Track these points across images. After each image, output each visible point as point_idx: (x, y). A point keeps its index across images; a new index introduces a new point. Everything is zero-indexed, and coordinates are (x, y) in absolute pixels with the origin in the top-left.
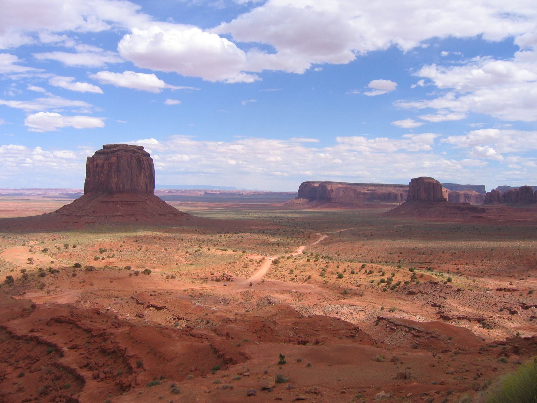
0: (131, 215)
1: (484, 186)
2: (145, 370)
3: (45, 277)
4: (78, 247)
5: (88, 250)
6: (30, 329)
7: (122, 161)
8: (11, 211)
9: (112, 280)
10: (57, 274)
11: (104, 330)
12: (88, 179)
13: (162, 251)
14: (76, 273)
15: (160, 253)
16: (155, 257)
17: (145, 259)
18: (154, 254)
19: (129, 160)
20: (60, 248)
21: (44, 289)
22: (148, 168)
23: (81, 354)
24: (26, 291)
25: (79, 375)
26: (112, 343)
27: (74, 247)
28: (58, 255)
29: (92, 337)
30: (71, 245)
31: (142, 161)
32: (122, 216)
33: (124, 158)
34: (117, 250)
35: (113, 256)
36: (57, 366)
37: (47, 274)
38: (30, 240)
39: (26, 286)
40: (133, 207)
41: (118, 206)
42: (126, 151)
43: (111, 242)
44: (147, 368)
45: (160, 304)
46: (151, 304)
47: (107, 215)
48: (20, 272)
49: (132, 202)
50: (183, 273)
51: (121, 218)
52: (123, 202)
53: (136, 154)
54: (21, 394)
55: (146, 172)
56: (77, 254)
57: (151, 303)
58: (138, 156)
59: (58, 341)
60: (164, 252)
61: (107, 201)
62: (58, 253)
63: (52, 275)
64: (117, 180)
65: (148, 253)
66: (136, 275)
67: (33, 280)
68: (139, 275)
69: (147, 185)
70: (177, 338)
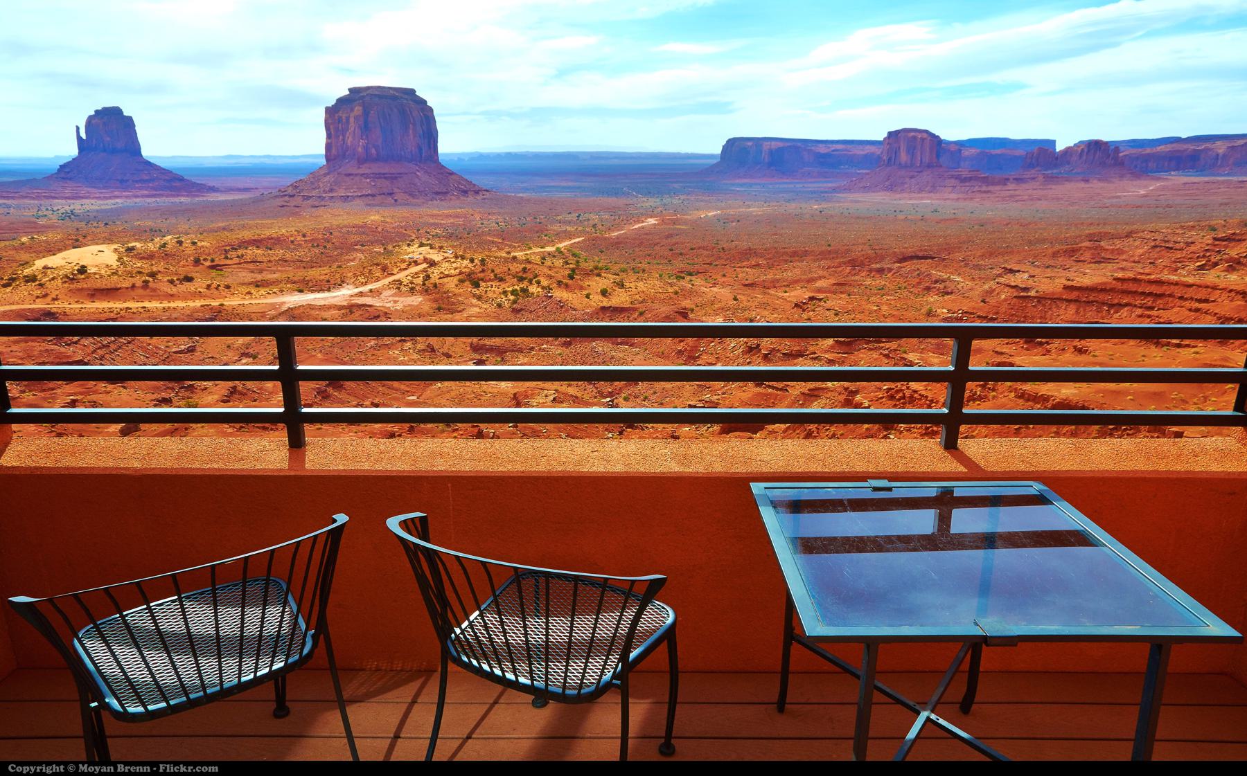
0: (388, 194)
1: (1054, 142)
12: (329, 141)
22: (422, 122)
31: (409, 113)
32: (373, 196)
40: (394, 181)
41: (368, 180)
51: (370, 198)
52: (376, 174)
61: (352, 174)
69: (420, 149)
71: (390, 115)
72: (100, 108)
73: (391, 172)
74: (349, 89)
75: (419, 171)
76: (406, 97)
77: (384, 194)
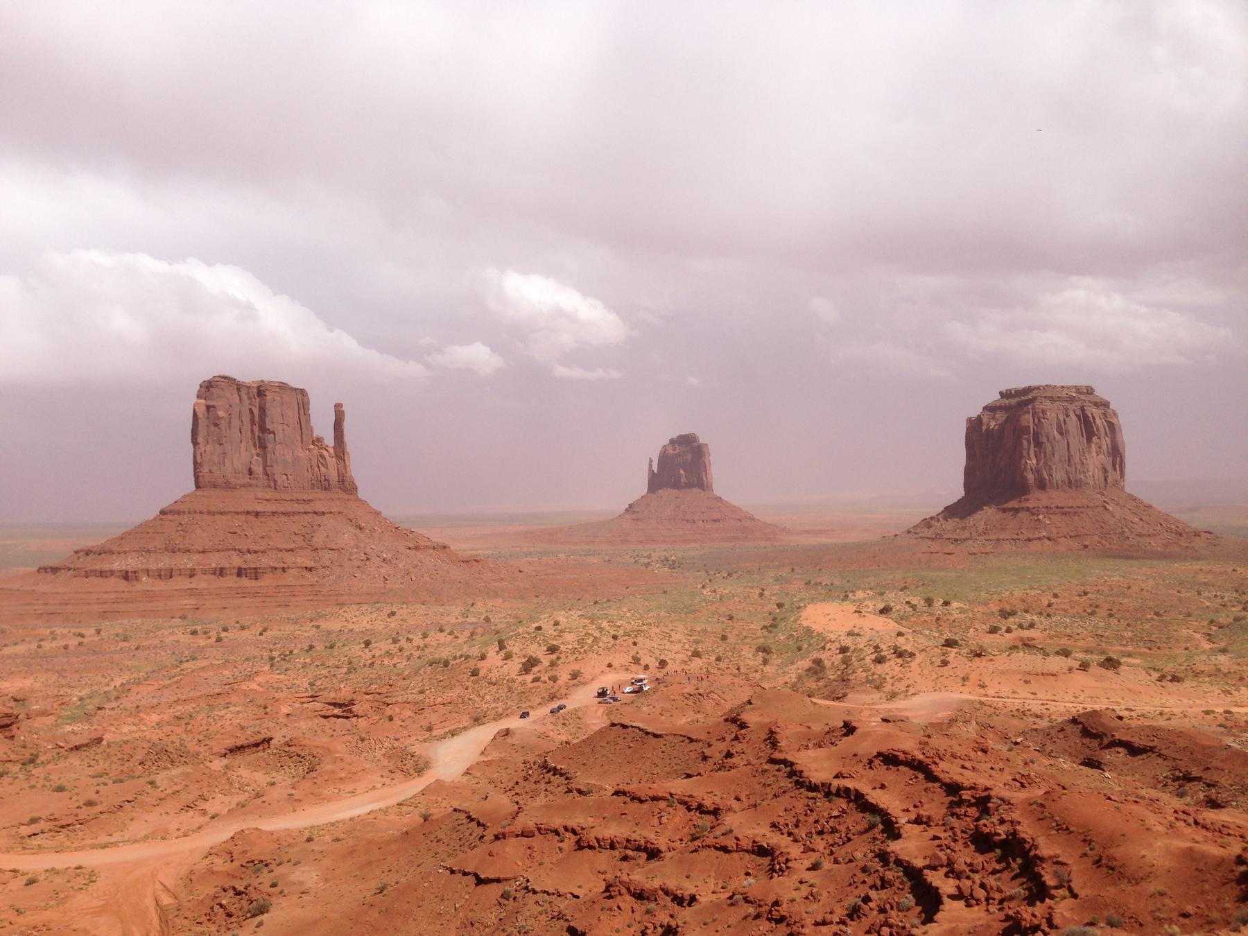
2: (1075, 896)
3: (887, 664)
4: (955, 605)
5: (976, 610)
6: (834, 774)
7: (1043, 421)
8: (821, 532)
9: (1028, 678)
10: (909, 659)
11: (986, 789)
13: (1149, 616)
14: (947, 659)
15: (1142, 623)
16: (1132, 632)
17: (1107, 634)
18: (1128, 625)
19: (1061, 417)
20: (916, 605)
21: (883, 689)
23: (935, 838)
24: (848, 691)
25: (931, 883)
26: (1002, 821)
27: (946, 603)
28: (913, 619)
29: (960, 803)
30: (939, 601)
32: (1049, 539)
33: (1048, 414)
34: (1041, 614)
35: (1032, 626)
36: (883, 857)
37: (888, 657)
38: (858, 589)
39: (848, 680)
40: (1076, 518)
41: (1041, 517)
42: (1051, 399)
43: (1027, 594)
44: (1082, 894)
45: (1137, 741)
46: (1117, 737)
47: (1016, 537)
48: (838, 652)
49: (1071, 507)
50: (1203, 671)
51: (1048, 542)
53: (1077, 404)
54: (814, 906)
55: (1104, 442)
56: (952, 618)
57: (1118, 736)
58: (1082, 409)
59: (889, 800)
60: (1152, 618)
62: (913, 615)
63: (900, 661)
64: (1034, 462)
65: (1114, 621)
66: (1084, 670)
67: (861, 670)
68: (1090, 670)
69: (1105, 471)
70: (1160, 828)
71: (1065, 423)
72: (675, 437)
73: (1070, 505)
74: (1001, 393)
75: (1108, 503)
76: (1083, 397)
77: (1065, 537)
